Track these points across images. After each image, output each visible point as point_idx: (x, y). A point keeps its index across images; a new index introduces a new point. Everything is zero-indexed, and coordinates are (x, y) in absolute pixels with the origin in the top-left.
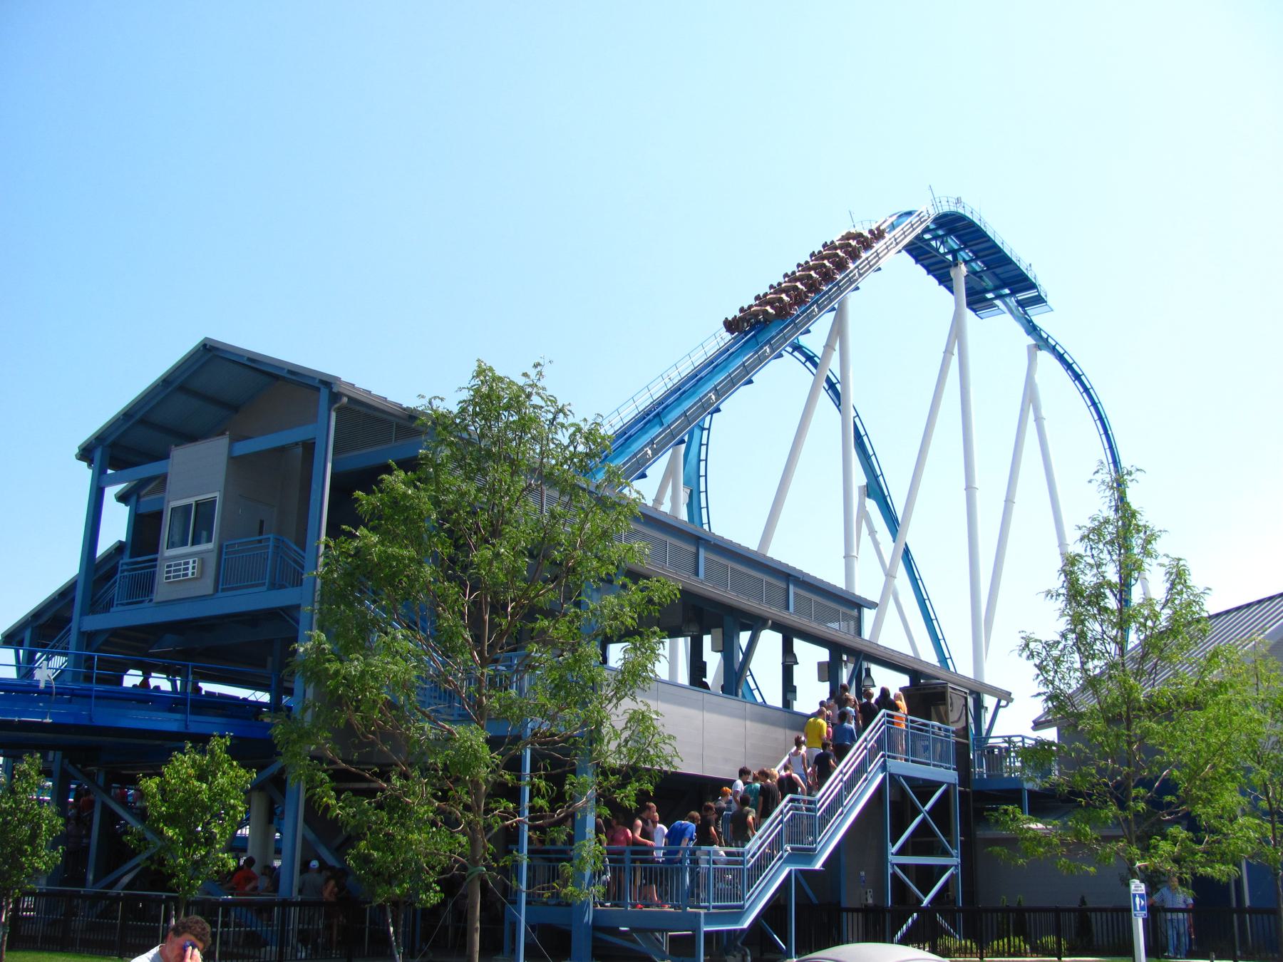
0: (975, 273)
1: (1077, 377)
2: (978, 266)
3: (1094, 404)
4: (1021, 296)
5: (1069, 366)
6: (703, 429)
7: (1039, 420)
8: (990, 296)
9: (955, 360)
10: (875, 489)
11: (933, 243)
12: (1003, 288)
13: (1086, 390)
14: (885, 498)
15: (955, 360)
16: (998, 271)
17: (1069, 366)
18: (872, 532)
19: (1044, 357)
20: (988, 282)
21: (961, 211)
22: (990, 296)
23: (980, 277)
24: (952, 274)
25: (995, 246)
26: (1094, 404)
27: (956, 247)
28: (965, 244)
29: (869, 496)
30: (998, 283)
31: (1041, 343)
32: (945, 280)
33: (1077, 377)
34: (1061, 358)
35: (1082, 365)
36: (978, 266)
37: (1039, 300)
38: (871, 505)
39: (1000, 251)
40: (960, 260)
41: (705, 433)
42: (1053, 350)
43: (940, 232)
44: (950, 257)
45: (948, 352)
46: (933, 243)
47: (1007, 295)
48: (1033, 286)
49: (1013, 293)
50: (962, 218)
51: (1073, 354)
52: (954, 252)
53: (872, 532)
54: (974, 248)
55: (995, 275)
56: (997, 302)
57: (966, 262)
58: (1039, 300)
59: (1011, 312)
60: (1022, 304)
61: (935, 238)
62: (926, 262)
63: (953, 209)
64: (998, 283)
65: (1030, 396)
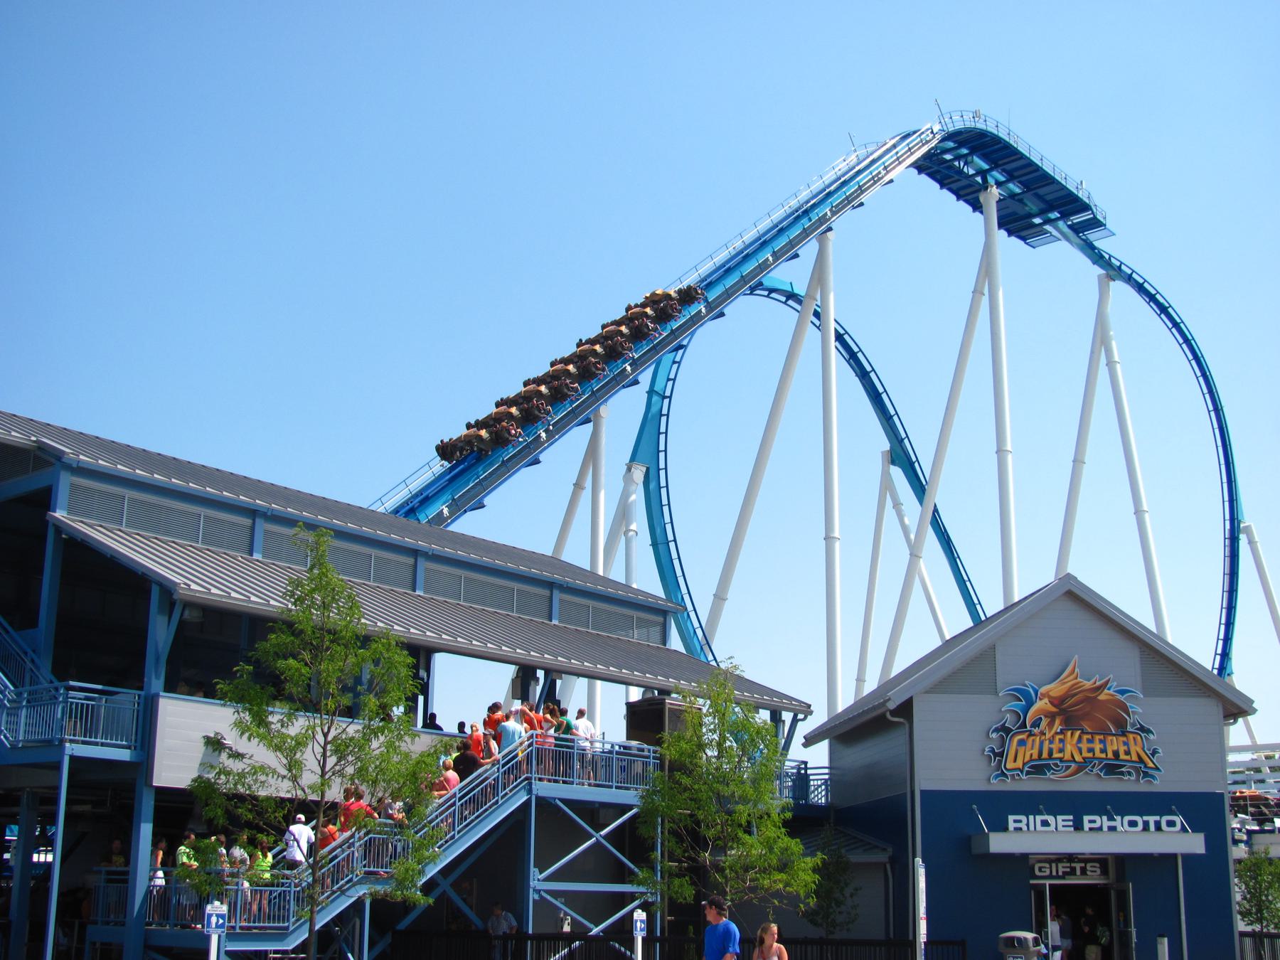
0: (1013, 196)
1: (1163, 309)
2: (1015, 188)
3: (1186, 341)
4: (1077, 219)
5: (1151, 298)
6: (664, 397)
7: (1110, 364)
8: (1037, 221)
9: (985, 301)
10: (900, 455)
11: (956, 163)
12: (1052, 209)
13: (1176, 325)
14: (912, 464)
15: (985, 301)
16: (1041, 191)
17: (1151, 298)
18: (897, 505)
19: (1119, 288)
20: (1032, 206)
21: (981, 125)
22: (1037, 221)
23: (1021, 201)
24: (982, 199)
25: (1031, 164)
26: (1186, 341)
27: (986, 167)
28: (995, 165)
29: (893, 463)
30: (1043, 206)
31: (1112, 273)
32: (977, 206)
33: (1163, 309)
34: (1140, 288)
35: (1168, 294)
36: (1015, 188)
37: (1095, 223)
38: (897, 473)
39: (1038, 169)
40: (991, 181)
41: (666, 401)
42: (1129, 279)
43: (965, 151)
44: (979, 179)
45: (977, 292)
46: (956, 163)
47: (1057, 219)
48: (1085, 207)
49: (1064, 216)
50: (983, 134)
51: (1156, 282)
52: (983, 173)
53: (897, 505)
54: (1008, 167)
55: (1037, 195)
56: (1047, 227)
57: (999, 184)
58: (1095, 223)
59: (1068, 239)
60: (1077, 229)
61: (958, 158)
62: (954, 186)
63: (968, 125)
64: (1043, 206)
65: (1101, 339)
